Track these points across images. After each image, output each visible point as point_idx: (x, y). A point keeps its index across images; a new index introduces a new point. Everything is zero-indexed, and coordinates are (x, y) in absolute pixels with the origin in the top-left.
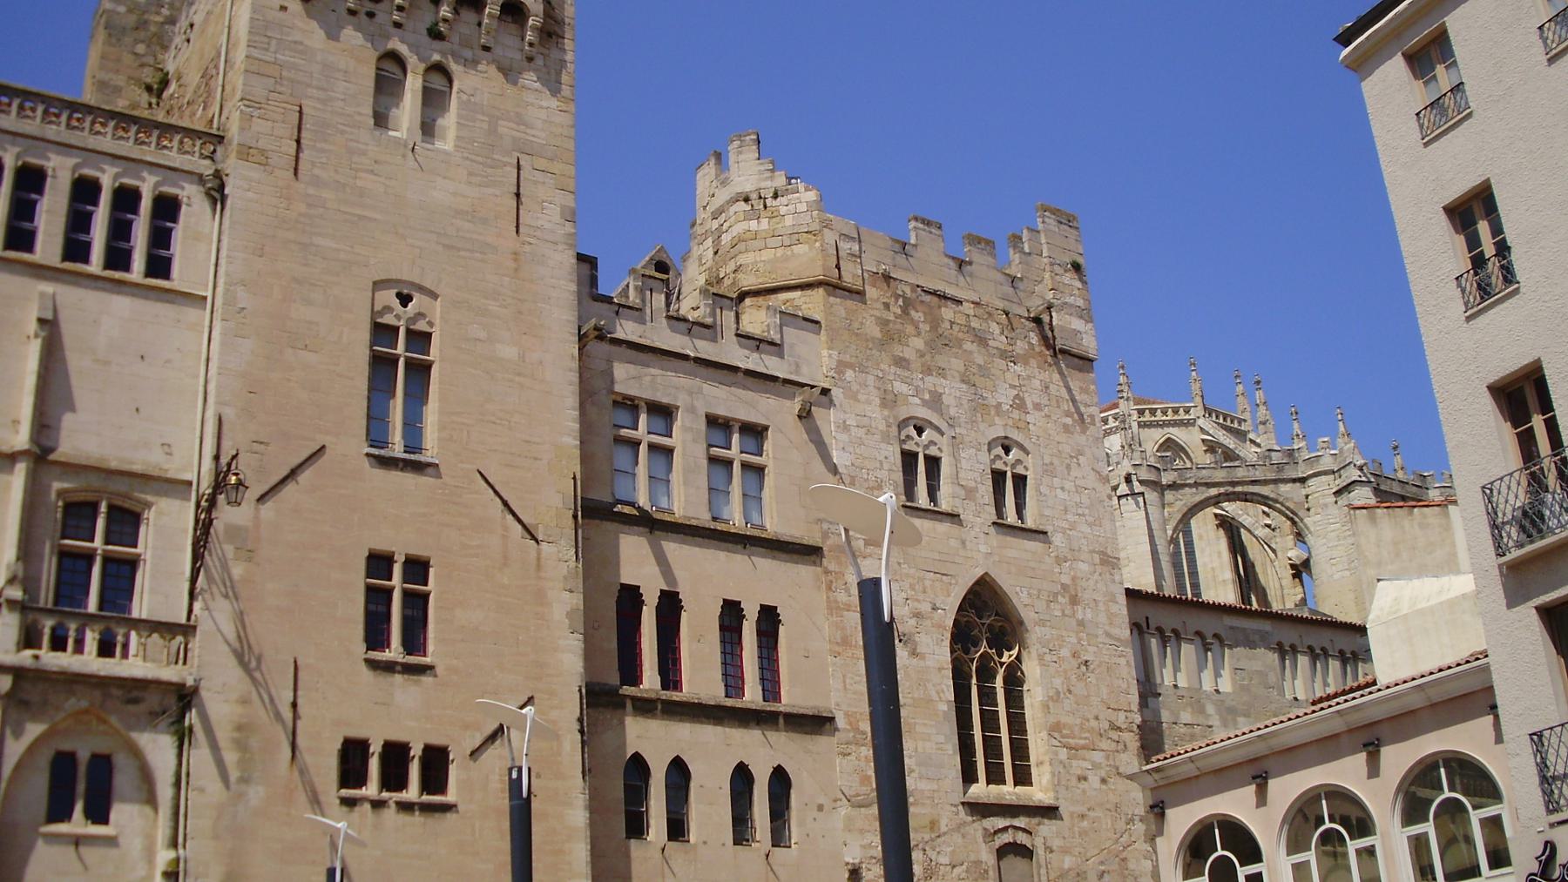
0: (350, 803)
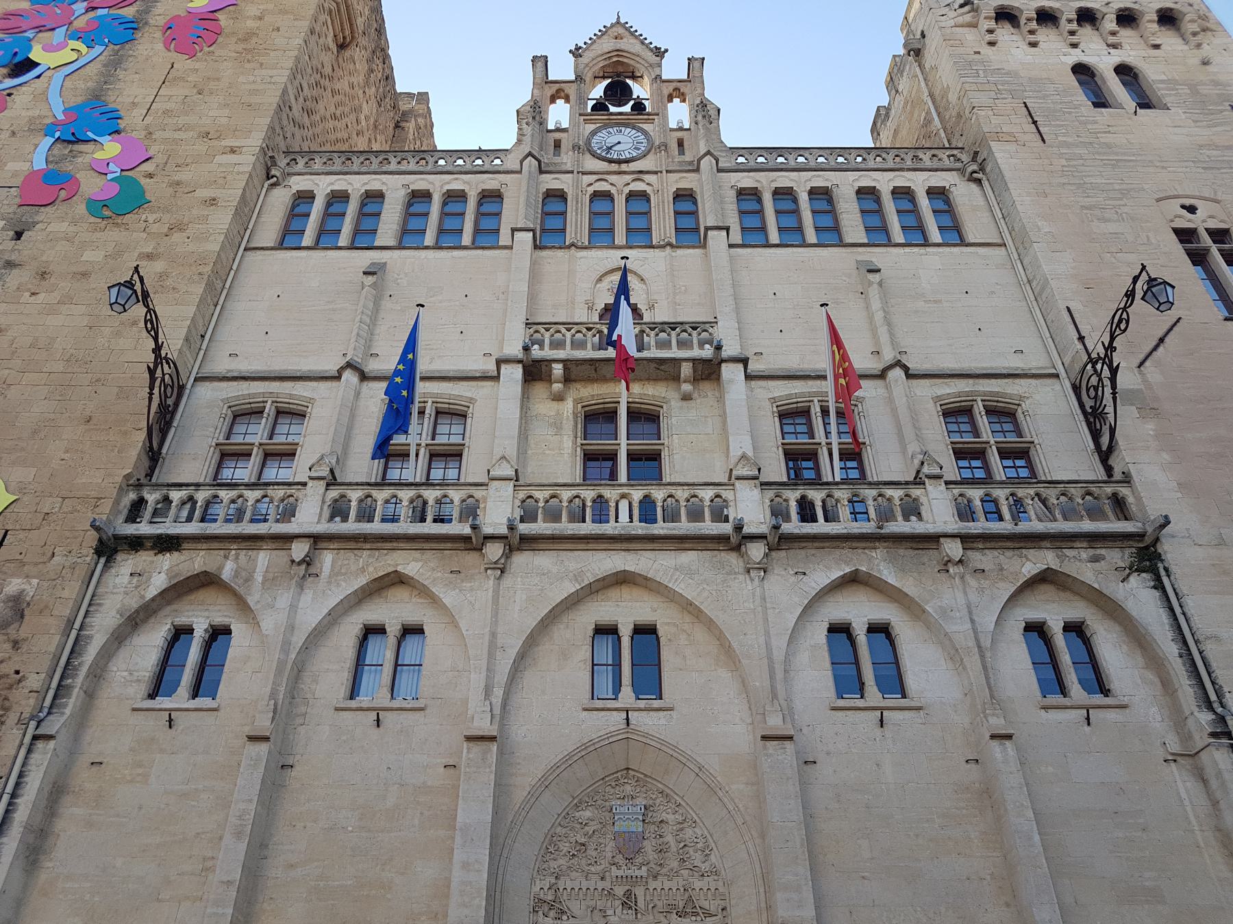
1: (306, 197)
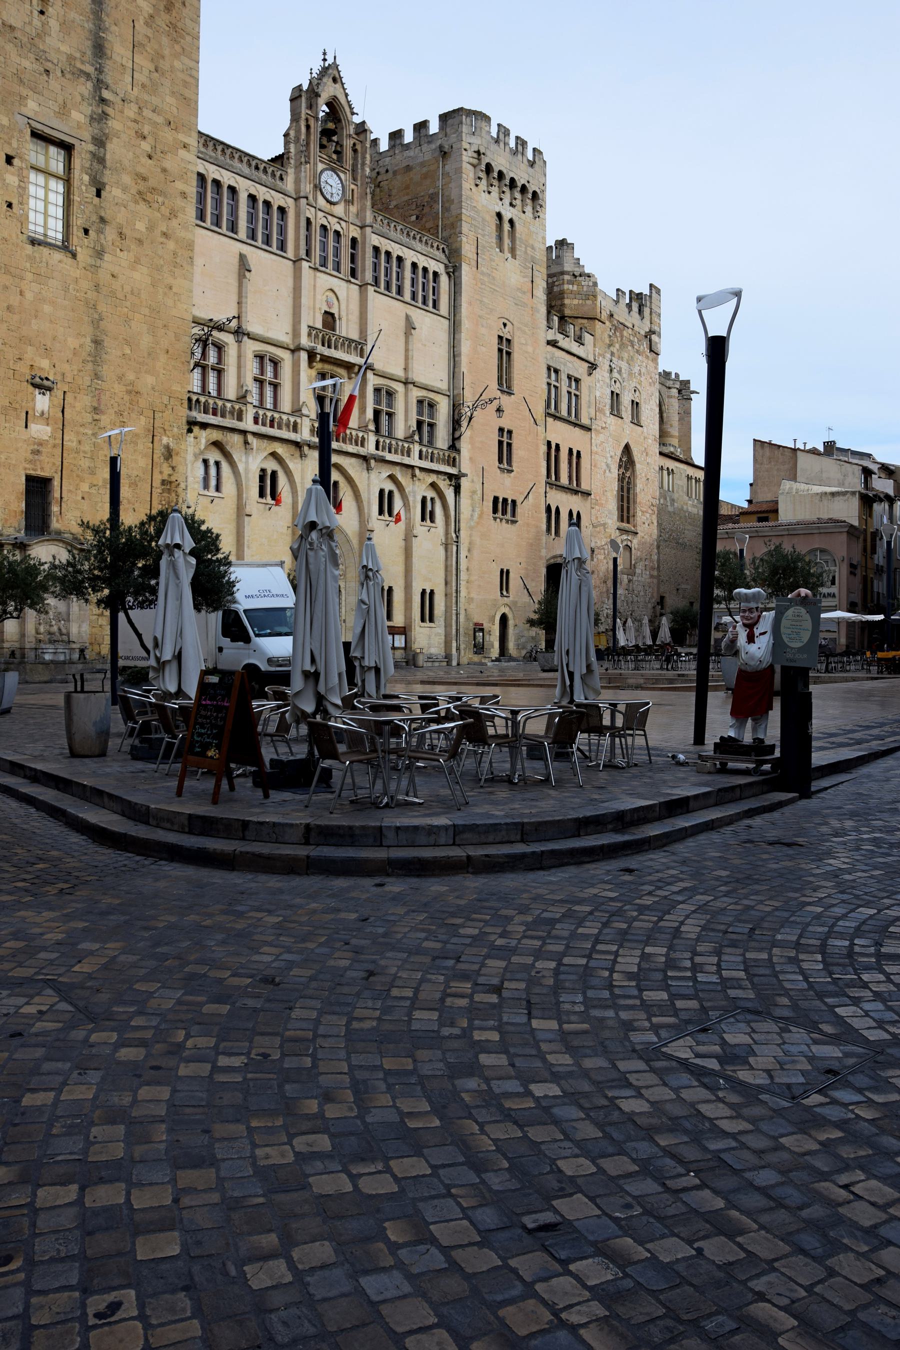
0: (495, 519)
1: (201, 177)
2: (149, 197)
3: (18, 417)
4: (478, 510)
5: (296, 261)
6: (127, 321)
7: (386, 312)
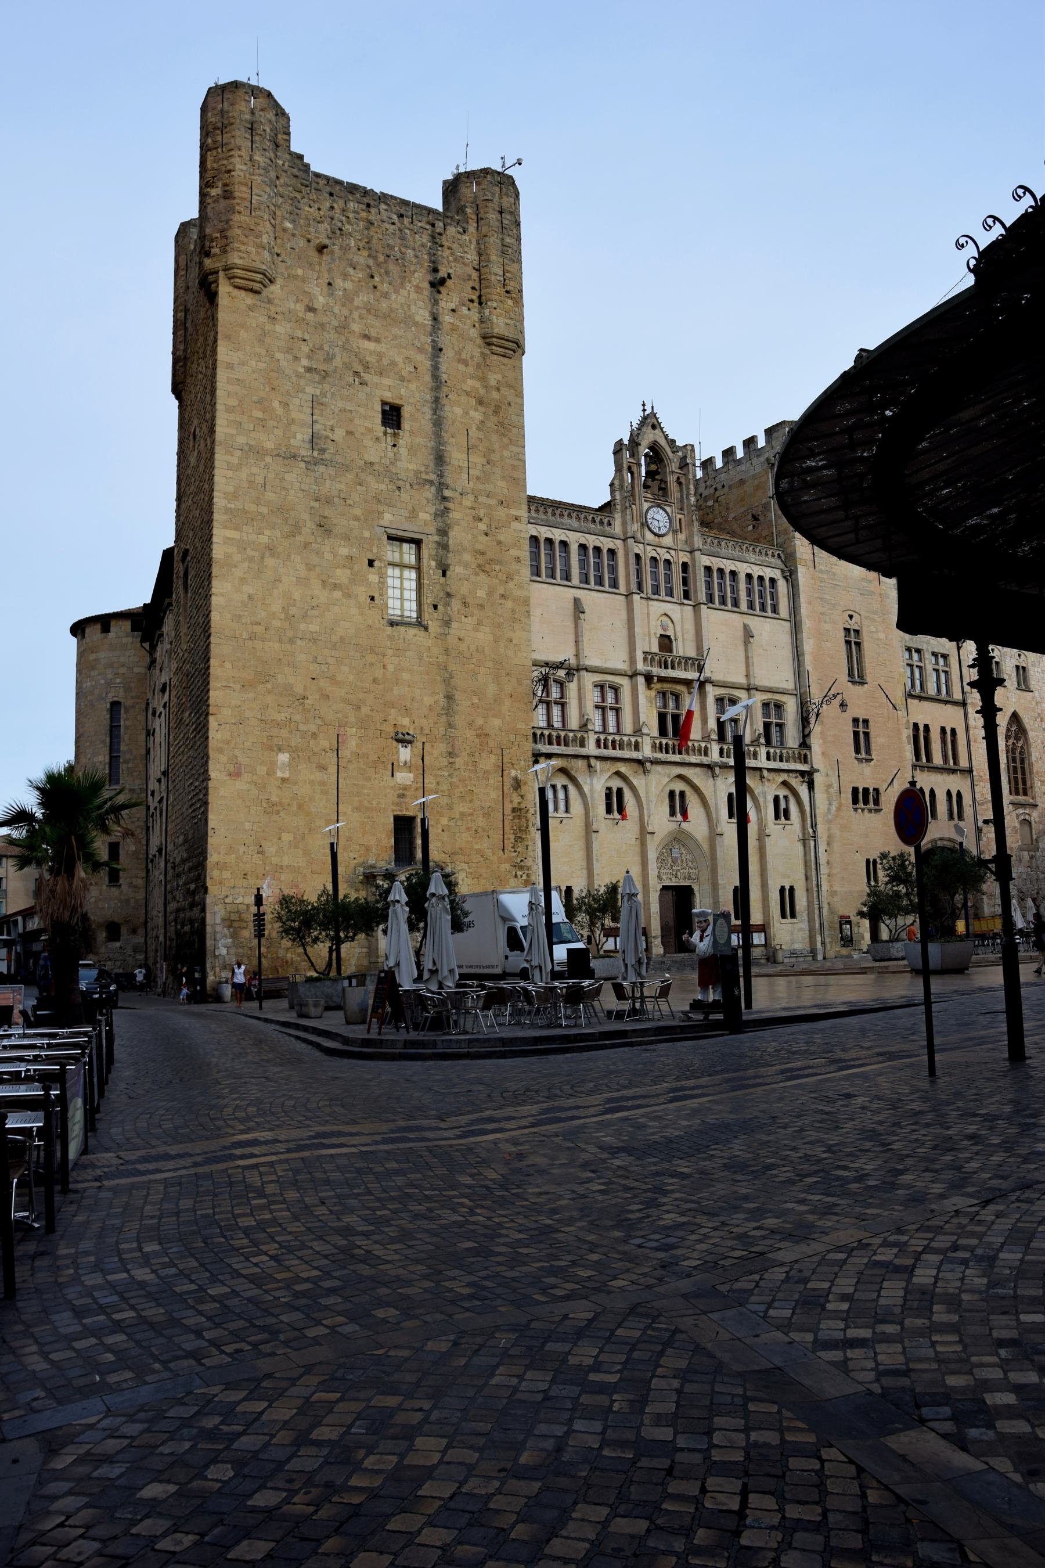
0: (856, 810)
1: (534, 540)
2: (487, 567)
3: (385, 768)
4: (835, 804)
5: (629, 595)
6: (474, 674)
7: (721, 626)
